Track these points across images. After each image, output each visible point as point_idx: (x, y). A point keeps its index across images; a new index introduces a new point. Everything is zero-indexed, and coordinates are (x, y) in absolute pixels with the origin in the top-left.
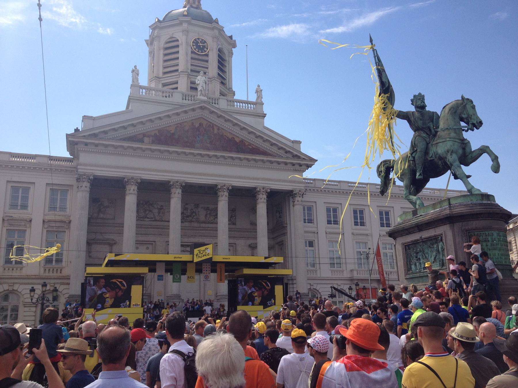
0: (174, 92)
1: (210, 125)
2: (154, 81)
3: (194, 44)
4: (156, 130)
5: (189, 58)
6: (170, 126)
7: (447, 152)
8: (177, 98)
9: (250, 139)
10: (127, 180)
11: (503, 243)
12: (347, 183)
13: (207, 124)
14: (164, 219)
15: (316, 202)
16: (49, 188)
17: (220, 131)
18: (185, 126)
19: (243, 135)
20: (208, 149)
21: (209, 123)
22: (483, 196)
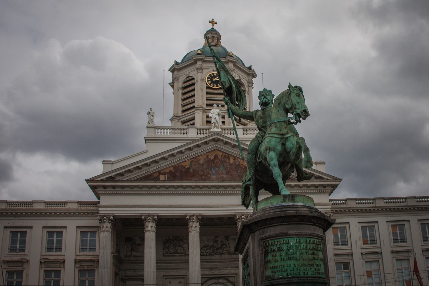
0: (188, 128)
1: (225, 156)
2: (174, 120)
4: (171, 166)
5: (205, 93)
6: (185, 161)
7: (266, 151)
8: (192, 134)
10: (144, 218)
11: (304, 251)
12: (355, 201)
13: (222, 155)
15: (349, 223)
18: (200, 160)
20: (223, 180)
21: (225, 154)
22: (286, 197)
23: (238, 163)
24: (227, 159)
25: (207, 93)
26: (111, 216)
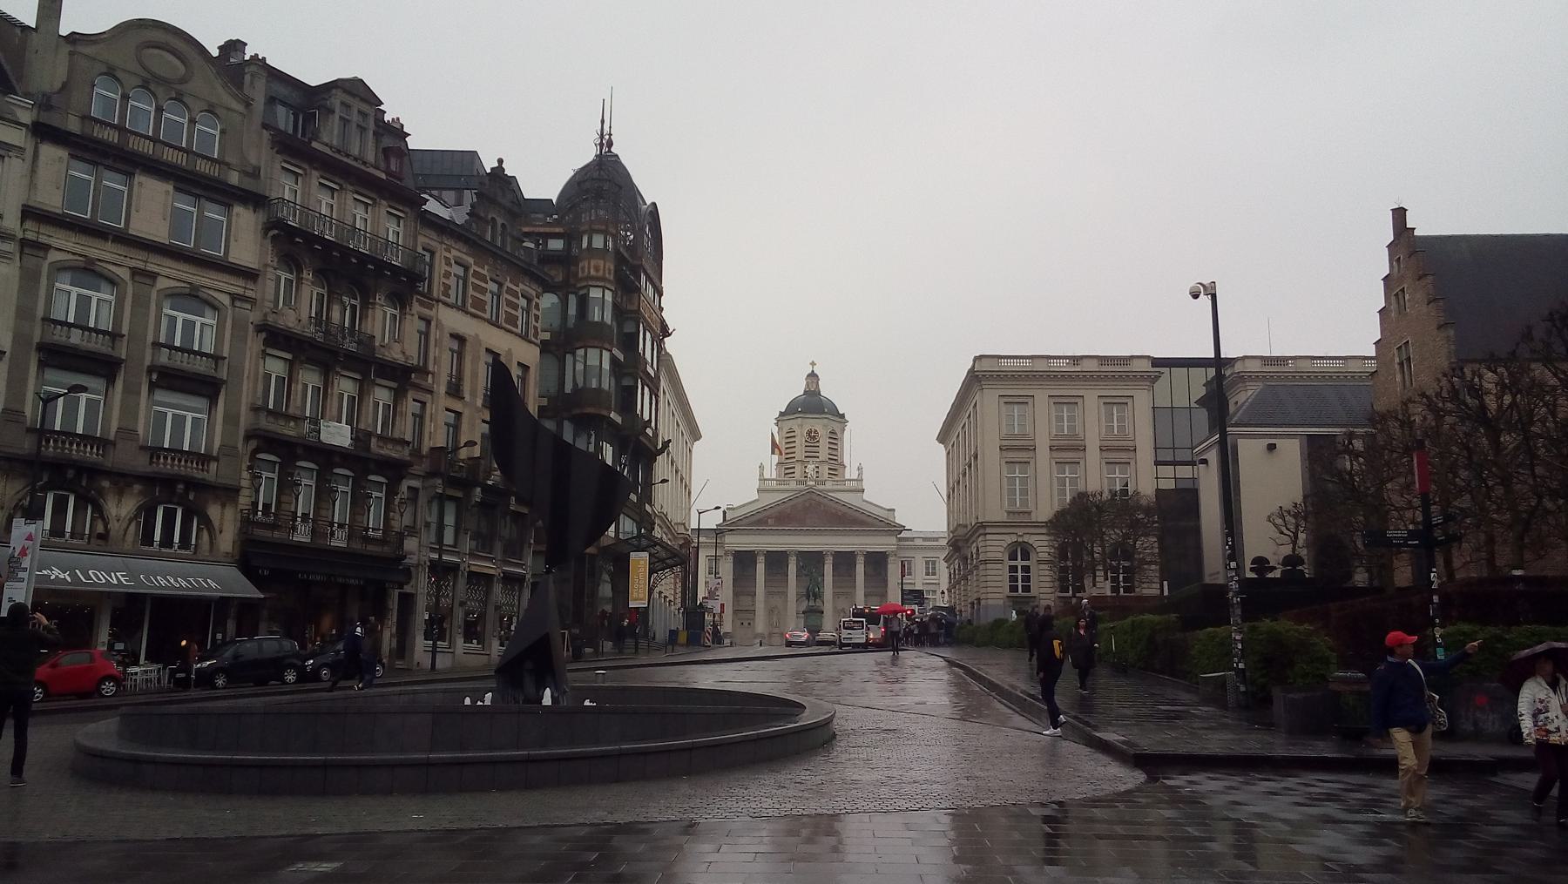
8: (793, 485)
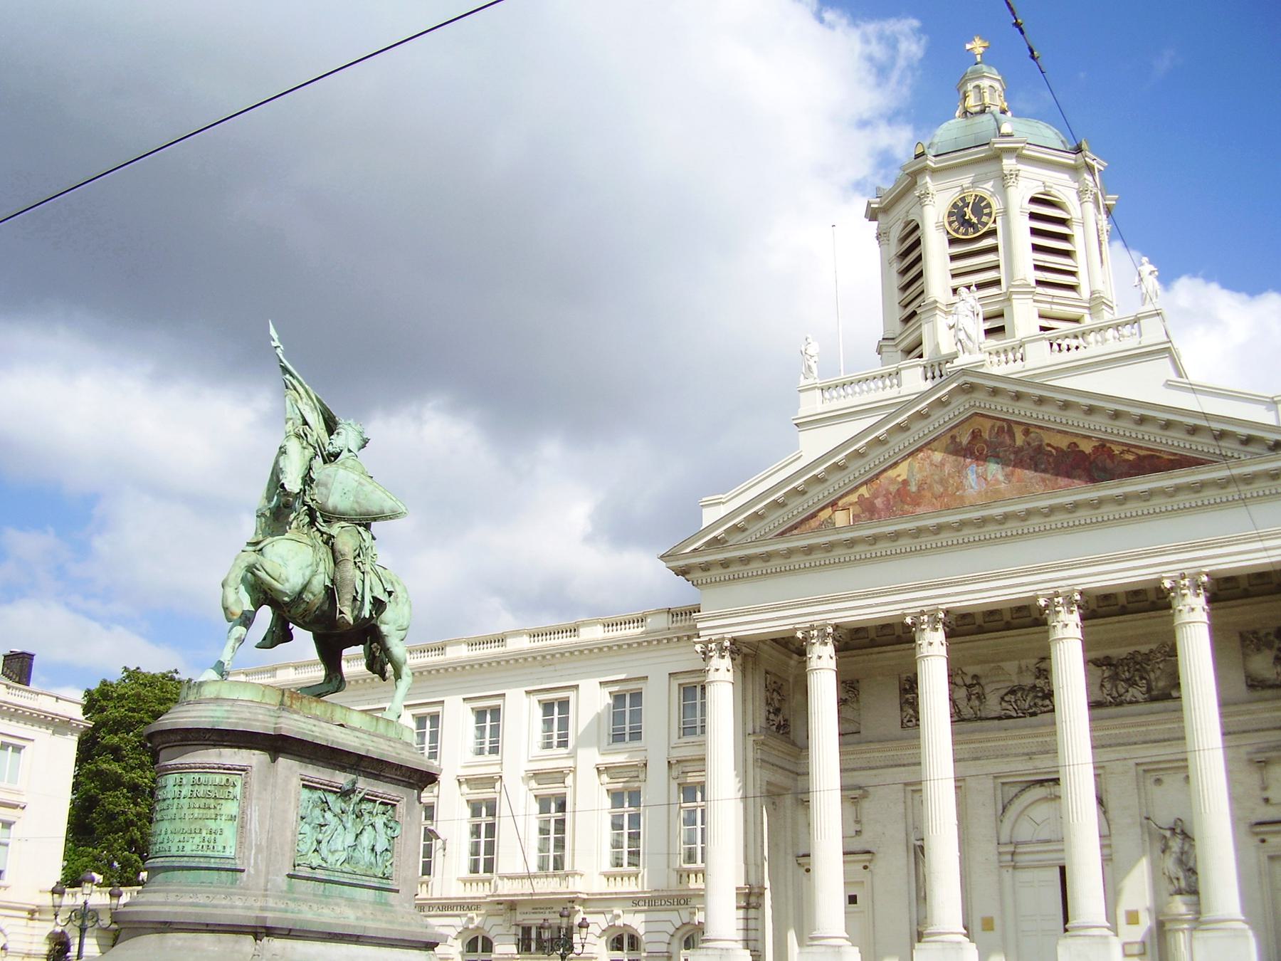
0: (900, 369)
1: (1001, 429)
3: (952, 219)
8: (914, 381)
9: (1123, 432)
13: (993, 427)
14: (983, 715)
16: (675, 684)
17: (1032, 435)
19: (1100, 427)
21: (999, 423)
23: (1036, 443)
24: (1007, 438)
25: (954, 258)
26: (723, 639)
